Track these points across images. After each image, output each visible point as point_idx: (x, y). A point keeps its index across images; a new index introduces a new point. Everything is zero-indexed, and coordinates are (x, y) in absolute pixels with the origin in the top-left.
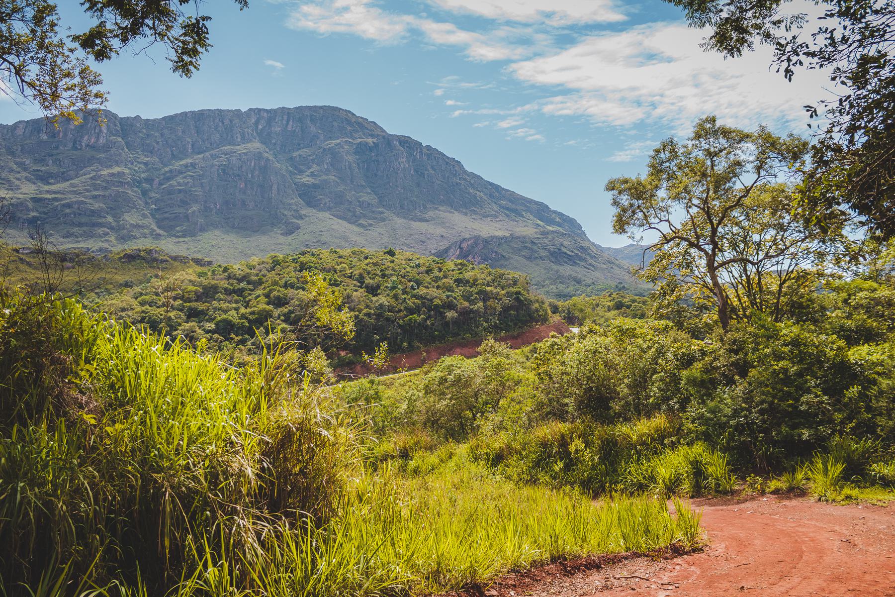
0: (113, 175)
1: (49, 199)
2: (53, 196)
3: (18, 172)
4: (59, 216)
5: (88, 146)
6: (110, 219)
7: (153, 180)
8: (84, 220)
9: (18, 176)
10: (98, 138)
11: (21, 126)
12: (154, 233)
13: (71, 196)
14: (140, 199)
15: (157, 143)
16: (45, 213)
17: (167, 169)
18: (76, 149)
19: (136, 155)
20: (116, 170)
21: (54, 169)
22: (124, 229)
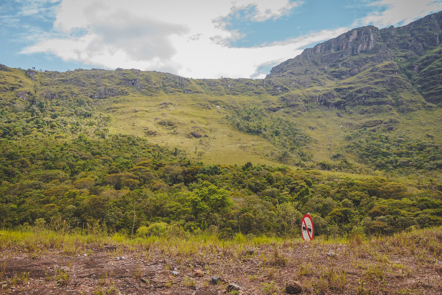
0: (386, 66)
1: (346, 89)
2: (348, 86)
3: (322, 75)
4: (354, 99)
5: (362, 51)
6: (390, 98)
7: (413, 67)
8: (372, 100)
9: (322, 77)
10: (368, 45)
11: (319, 47)
12: (426, 106)
13: (360, 85)
14: (408, 81)
15: (410, 41)
16: (344, 98)
17: (424, 57)
18: (354, 55)
19: (396, 52)
20: (386, 63)
21: (344, 69)
22: (402, 104)
